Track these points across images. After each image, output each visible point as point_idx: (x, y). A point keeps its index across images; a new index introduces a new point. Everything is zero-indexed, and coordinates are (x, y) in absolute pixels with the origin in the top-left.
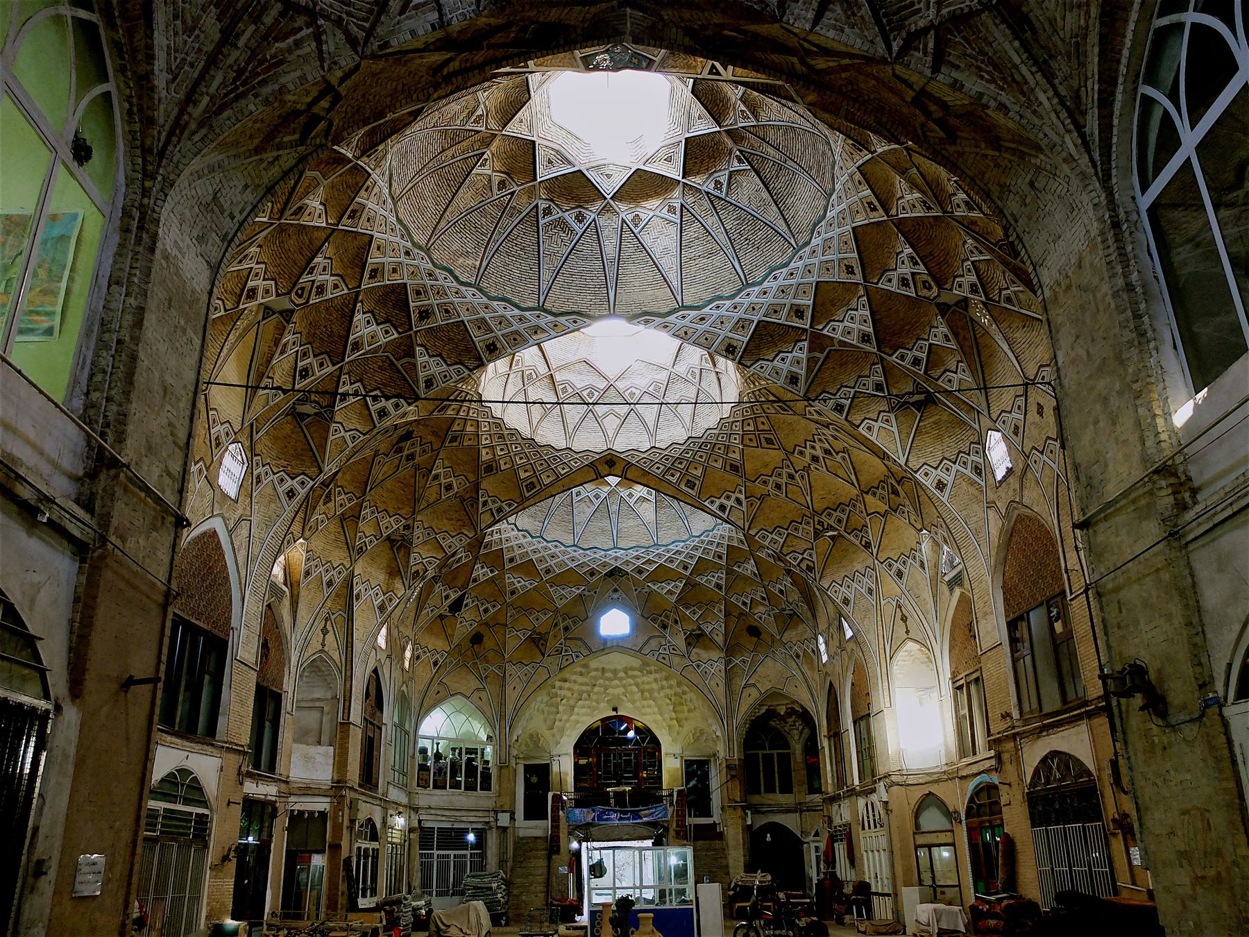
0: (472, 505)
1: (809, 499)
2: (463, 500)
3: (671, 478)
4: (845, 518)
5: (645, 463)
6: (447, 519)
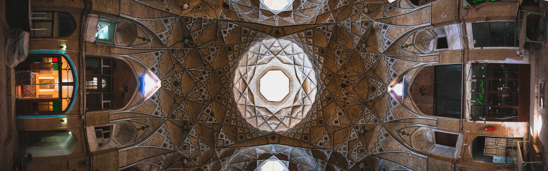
0: (333, 37)
1: (200, 53)
2: (336, 41)
3: (253, 32)
4: (185, 53)
5: (264, 36)
6: (344, 35)
